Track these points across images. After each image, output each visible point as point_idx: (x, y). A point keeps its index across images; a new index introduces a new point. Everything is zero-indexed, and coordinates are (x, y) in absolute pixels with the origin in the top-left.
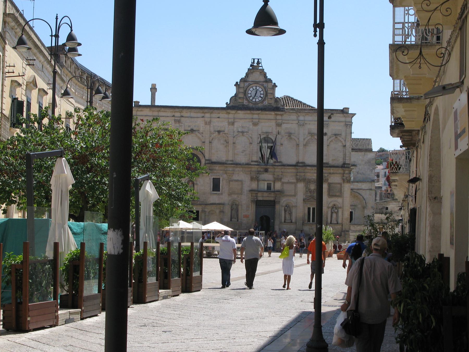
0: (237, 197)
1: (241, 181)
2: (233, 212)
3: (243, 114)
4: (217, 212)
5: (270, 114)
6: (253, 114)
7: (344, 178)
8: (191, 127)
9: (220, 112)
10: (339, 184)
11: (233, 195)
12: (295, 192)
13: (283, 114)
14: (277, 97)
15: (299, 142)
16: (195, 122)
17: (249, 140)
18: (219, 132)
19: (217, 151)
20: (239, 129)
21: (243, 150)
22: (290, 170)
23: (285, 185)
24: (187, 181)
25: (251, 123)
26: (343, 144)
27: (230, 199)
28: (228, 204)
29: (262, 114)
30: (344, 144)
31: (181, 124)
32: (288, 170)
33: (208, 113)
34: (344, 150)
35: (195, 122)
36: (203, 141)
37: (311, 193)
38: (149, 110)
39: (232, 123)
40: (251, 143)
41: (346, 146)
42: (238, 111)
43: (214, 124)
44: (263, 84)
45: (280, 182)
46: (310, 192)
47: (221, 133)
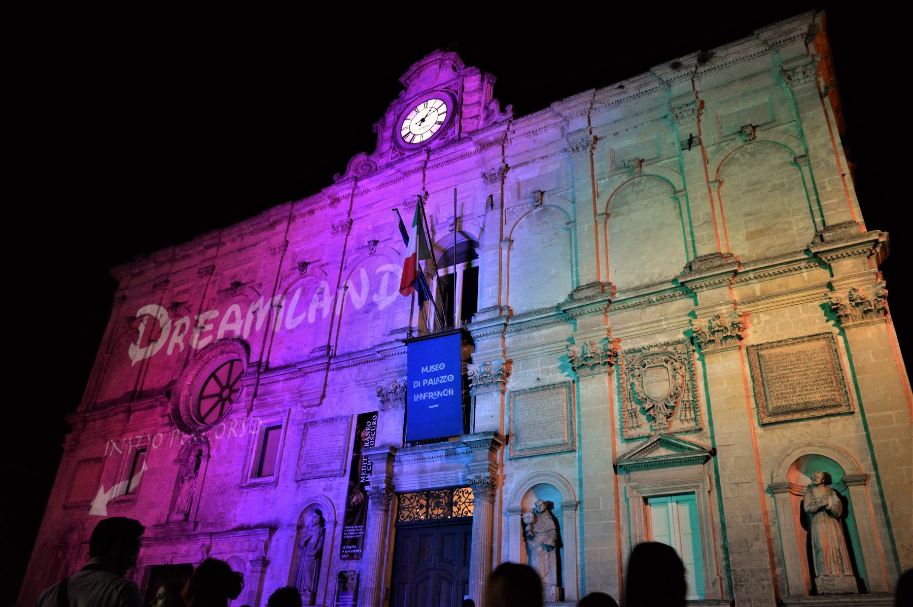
0: (324, 489)
2: (307, 563)
5: (462, 157)
6: (407, 174)
7: (841, 296)
8: (236, 279)
9: (315, 206)
10: (811, 337)
12: (571, 433)
15: (575, 215)
16: (249, 258)
22: (545, 332)
23: (520, 402)
26: (791, 153)
27: (299, 500)
29: (437, 166)
30: (799, 151)
31: (213, 278)
32: (535, 334)
34: (808, 177)
35: (249, 258)
38: (153, 265)
41: (811, 152)
42: (359, 184)
43: (296, 250)
44: (447, 88)
45: (495, 394)
46: (650, 413)
47: (309, 267)
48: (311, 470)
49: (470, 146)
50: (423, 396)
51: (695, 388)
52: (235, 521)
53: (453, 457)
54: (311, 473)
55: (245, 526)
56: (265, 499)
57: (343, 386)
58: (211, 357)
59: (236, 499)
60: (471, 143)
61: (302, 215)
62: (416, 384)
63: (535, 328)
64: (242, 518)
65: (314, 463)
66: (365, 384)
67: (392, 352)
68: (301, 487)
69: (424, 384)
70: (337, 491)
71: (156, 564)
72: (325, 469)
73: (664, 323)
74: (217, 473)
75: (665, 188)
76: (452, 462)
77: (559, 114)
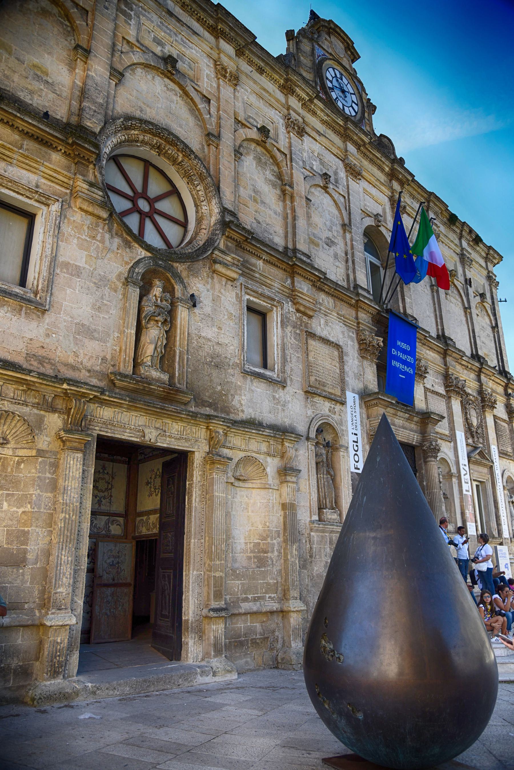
1: (337, 346)
3: (323, 122)
4: (268, 470)
9: (267, 69)
11: (317, 399)
13: (408, 180)
14: (381, 135)
17: (341, 213)
18: (263, 130)
19: (255, 201)
20: (314, 163)
21: (328, 238)
24: (140, 270)
25: (341, 164)
26: (491, 321)
28: (308, 438)
29: (365, 155)
32: (428, 352)
33: (229, 40)
36: (212, 127)
37: (473, 437)
39: (299, 128)
40: (346, 227)
42: (316, 101)
48: (318, 386)
49: (388, 166)
50: (398, 364)
51: (482, 426)
52: (243, 411)
53: (410, 421)
54: (318, 388)
55: (257, 422)
56: (274, 397)
57: (327, 311)
58: (141, 137)
59: (239, 383)
60: (390, 165)
61: (250, 63)
62: (394, 352)
63: (429, 348)
64: (251, 410)
65: (321, 379)
66: (344, 321)
67: (366, 307)
68: (309, 400)
69: (399, 355)
70: (340, 417)
71: (123, 437)
72: (330, 391)
73: (471, 383)
74: (203, 334)
75: (460, 300)
76: (407, 424)
77: (428, 202)
